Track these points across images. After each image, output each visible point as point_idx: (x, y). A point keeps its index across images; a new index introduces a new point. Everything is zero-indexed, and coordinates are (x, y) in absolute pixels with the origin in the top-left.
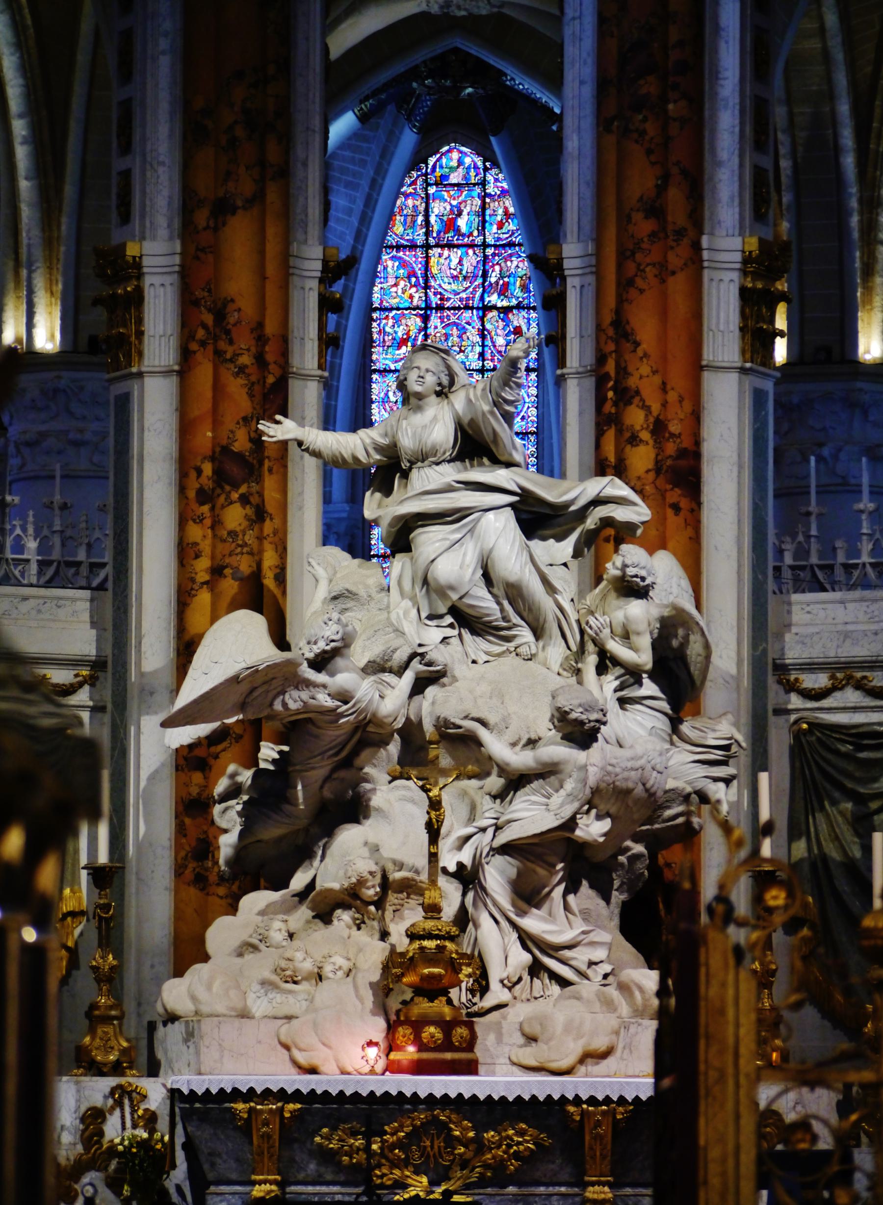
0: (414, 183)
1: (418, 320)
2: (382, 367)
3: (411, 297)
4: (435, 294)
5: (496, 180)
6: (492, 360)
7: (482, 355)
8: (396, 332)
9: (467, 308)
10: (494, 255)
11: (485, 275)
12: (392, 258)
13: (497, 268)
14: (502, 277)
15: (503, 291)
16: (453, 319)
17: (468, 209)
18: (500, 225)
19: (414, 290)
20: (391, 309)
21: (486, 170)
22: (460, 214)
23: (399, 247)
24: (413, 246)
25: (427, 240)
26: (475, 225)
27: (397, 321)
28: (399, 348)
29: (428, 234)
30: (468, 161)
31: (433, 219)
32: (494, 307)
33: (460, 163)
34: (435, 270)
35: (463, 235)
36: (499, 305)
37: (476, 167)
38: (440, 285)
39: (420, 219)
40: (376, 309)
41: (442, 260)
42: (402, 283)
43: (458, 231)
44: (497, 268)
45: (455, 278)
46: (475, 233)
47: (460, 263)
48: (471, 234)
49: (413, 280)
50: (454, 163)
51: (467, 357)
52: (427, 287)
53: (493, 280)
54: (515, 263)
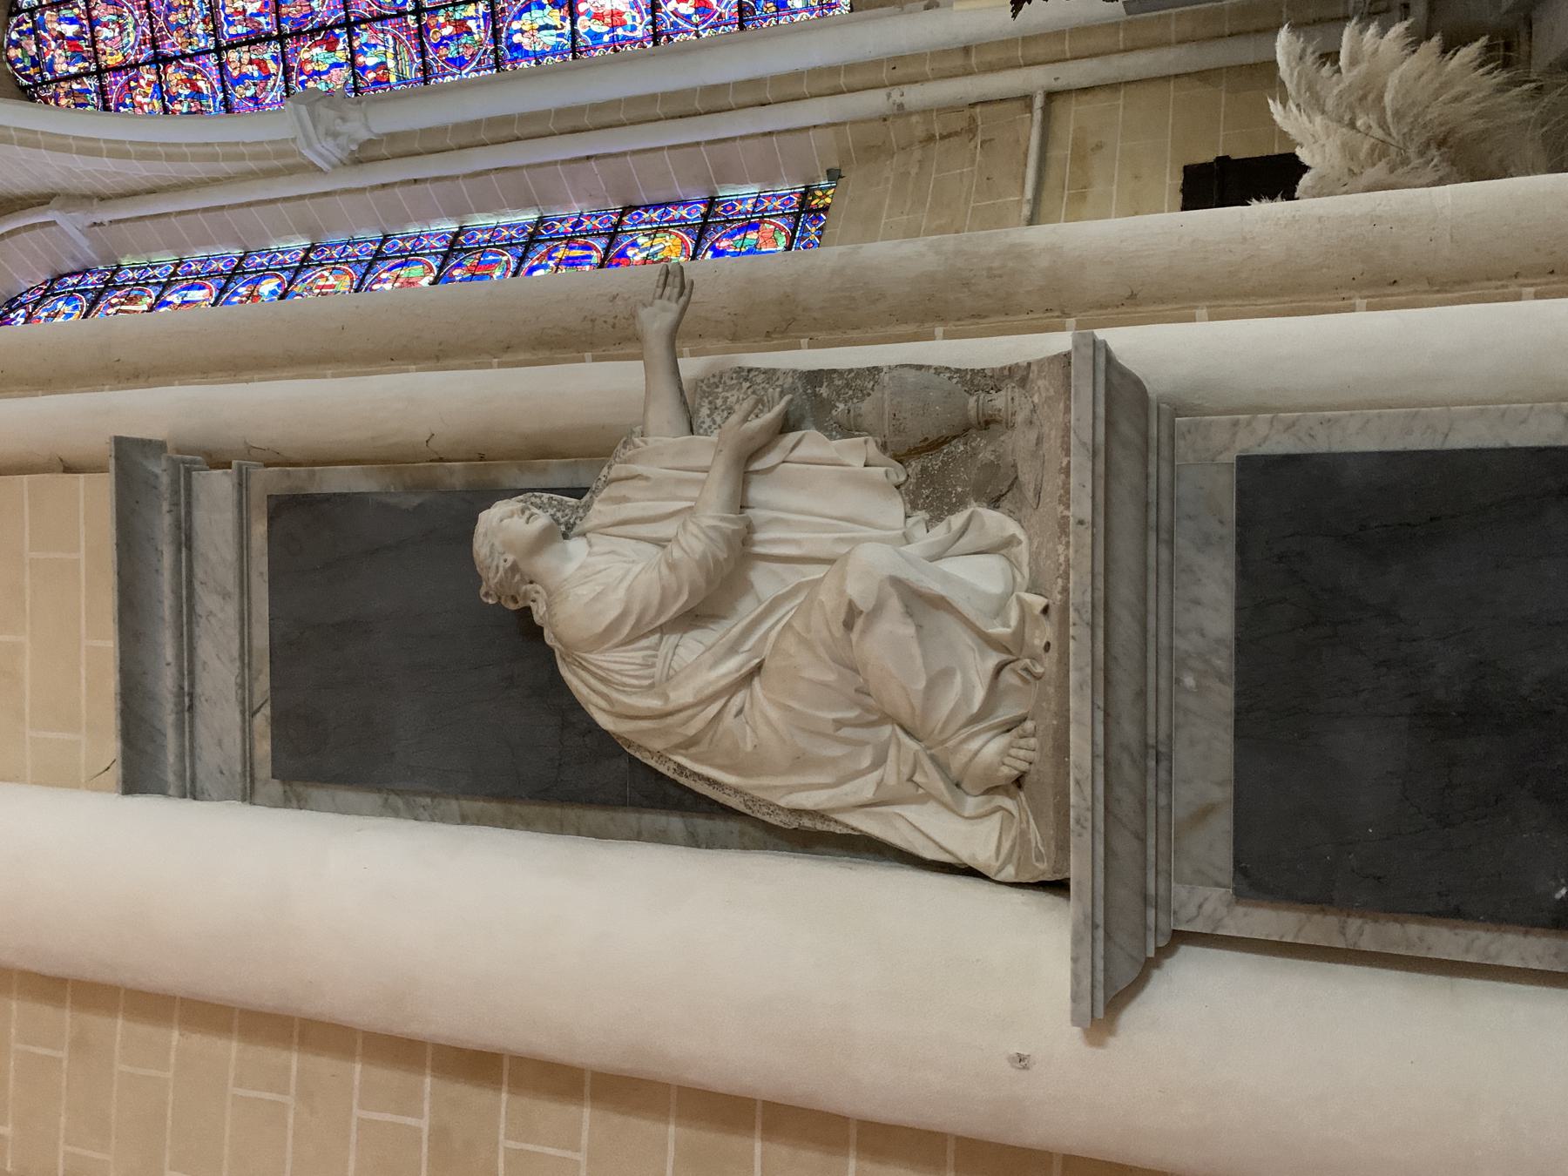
1: (170, 70)
3: (149, 84)
16: (161, 24)
19: (142, 82)
22: (62, 35)
29: (88, 74)
31: (73, 70)
33: (17, 44)
34: (119, 58)
37: (19, 24)
39: (75, 86)
41: (108, 50)
42: (139, 98)
43: (78, 37)
47: (106, 25)
50: (19, 52)
52: (136, 65)
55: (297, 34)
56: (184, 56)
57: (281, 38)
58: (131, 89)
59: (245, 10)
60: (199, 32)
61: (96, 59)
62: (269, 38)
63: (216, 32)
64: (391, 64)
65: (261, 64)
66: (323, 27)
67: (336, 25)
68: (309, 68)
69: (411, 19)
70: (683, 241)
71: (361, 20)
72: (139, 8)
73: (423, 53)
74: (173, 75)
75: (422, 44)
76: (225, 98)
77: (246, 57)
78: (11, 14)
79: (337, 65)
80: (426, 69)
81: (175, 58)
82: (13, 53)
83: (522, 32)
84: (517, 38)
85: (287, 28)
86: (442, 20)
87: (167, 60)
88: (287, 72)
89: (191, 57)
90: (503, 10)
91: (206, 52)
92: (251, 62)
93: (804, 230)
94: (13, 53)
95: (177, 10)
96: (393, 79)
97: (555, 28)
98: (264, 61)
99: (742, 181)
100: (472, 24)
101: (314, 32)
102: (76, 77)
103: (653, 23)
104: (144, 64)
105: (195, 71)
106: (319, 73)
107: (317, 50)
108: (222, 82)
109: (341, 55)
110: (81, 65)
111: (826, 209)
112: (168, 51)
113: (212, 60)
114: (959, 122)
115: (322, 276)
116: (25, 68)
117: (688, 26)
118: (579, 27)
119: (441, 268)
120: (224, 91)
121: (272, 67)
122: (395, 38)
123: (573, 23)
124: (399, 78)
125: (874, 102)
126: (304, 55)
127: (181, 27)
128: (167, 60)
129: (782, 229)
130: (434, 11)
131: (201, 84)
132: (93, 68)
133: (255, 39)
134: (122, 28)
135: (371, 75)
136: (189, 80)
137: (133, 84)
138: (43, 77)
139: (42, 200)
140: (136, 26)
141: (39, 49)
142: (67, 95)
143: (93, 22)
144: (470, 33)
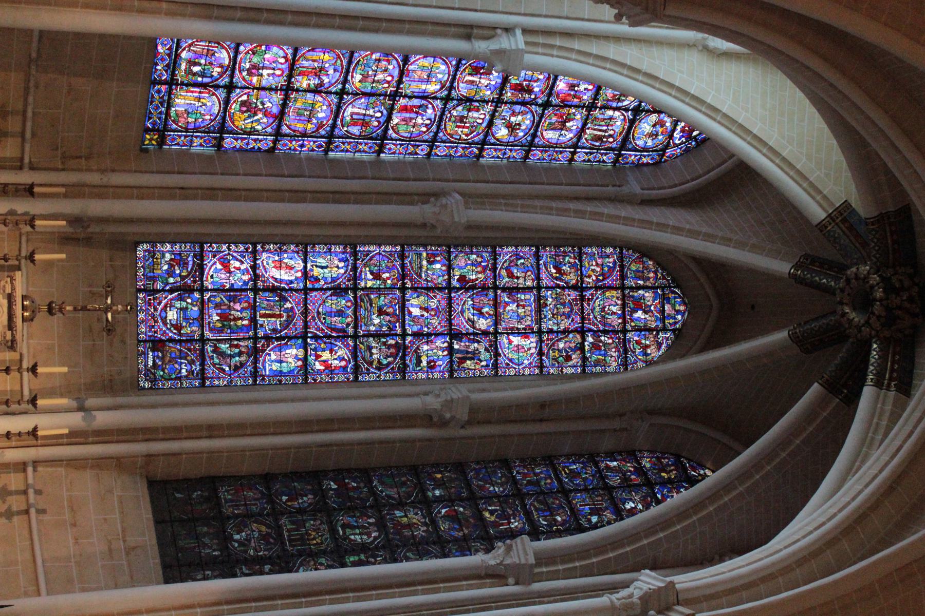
0: (664, 278)
2: (541, 254)
3: (589, 276)
4: (592, 295)
5: (667, 339)
6: (548, 339)
7: (550, 331)
8: (565, 265)
9: (583, 319)
10: (619, 338)
11: (605, 332)
12: (614, 261)
13: (610, 341)
14: (605, 344)
15: (595, 346)
16: (575, 308)
17: (649, 318)
18: (638, 343)
19: (594, 278)
20: (581, 261)
21: (673, 331)
22: (645, 312)
23: (622, 267)
24: (623, 277)
25: (628, 288)
26: (638, 324)
27: (572, 266)
28: (555, 267)
29: (632, 289)
30: (679, 317)
31: (641, 292)
32: (584, 340)
33: (678, 312)
34: (608, 294)
35: (631, 315)
36: (586, 343)
37: (675, 323)
38: (597, 298)
40: (580, 249)
41: (614, 299)
42: (598, 269)
43: (634, 311)
44: (610, 341)
45: (603, 309)
46: (633, 324)
48: (632, 321)
49: (601, 278)
50: (677, 307)
51: (550, 320)
52: (597, 288)
53: (603, 338)
54: (614, 355)
55: (484, 288)
56: (563, 288)
57: (495, 288)
58: (603, 274)
59: (518, 306)
60: (550, 300)
61: (624, 296)
62: (504, 289)
63: (539, 298)
64: (425, 263)
65: (511, 275)
66: (467, 290)
67: (458, 289)
68: (479, 269)
69: (409, 285)
70: (233, 123)
71: (441, 289)
72: (589, 319)
73: (403, 266)
74: (572, 279)
75: (403, 271)
76: (538, 260)
77: (521, 281)
78: (679, 330)
79: (460, 268)
80: (402, 257)
81: (569, 288)
82: (682, 308)
83: (338, 267)
84: (341, 264)
85: (491, 294)
86: (389, 282)
87: (574, 287)
88: (494, 269)
89: (558, 286)
90: (349, 280)
91: (548, 288)
92: (518, 278)
93: (160, 118)
94: (682, 308)
95: (563, 314)
96: (424, 254)
97: (317, 266)
98: (509, 277)
99: (199, 155)
100: (370, 277)
101: (473, 287)
102: (639, 288)
103: (255, 259)
104: (591, 288)
105: (556, 278)
106: (472, 265)
107: (474, 277)
108: (539, 269)
109: (457, 273)
110: (636, 294)
111: (147, 130)
112: (574, 294)
113: (545, 282)
114: (72, 163)
115: (467, 135)
116: (675, 298)
117: (235, 254)
118: (302, 265)
119: (387, 129)
120: (538, 265)
121: (504, 273)
122: (420, 277)
123: (305, 267)
124: (421, 255)
125: (118, 179)
126: (481, 276)
127: (561, 304)
128: (574, 287)
129: (174, 121)
130: (392, 288)
131: (554, 271)
132: (627, 292)
133: (512, 291)
134: (603, 309)
135: (438, 259)
136: (562, 274)
137: (601, 278)
138: (663, 291)
139: (647, 202)
140: (593, 310)
141: (664, 308)
142: (649, 279)
143: (623, 316)
144: (372, 273)
